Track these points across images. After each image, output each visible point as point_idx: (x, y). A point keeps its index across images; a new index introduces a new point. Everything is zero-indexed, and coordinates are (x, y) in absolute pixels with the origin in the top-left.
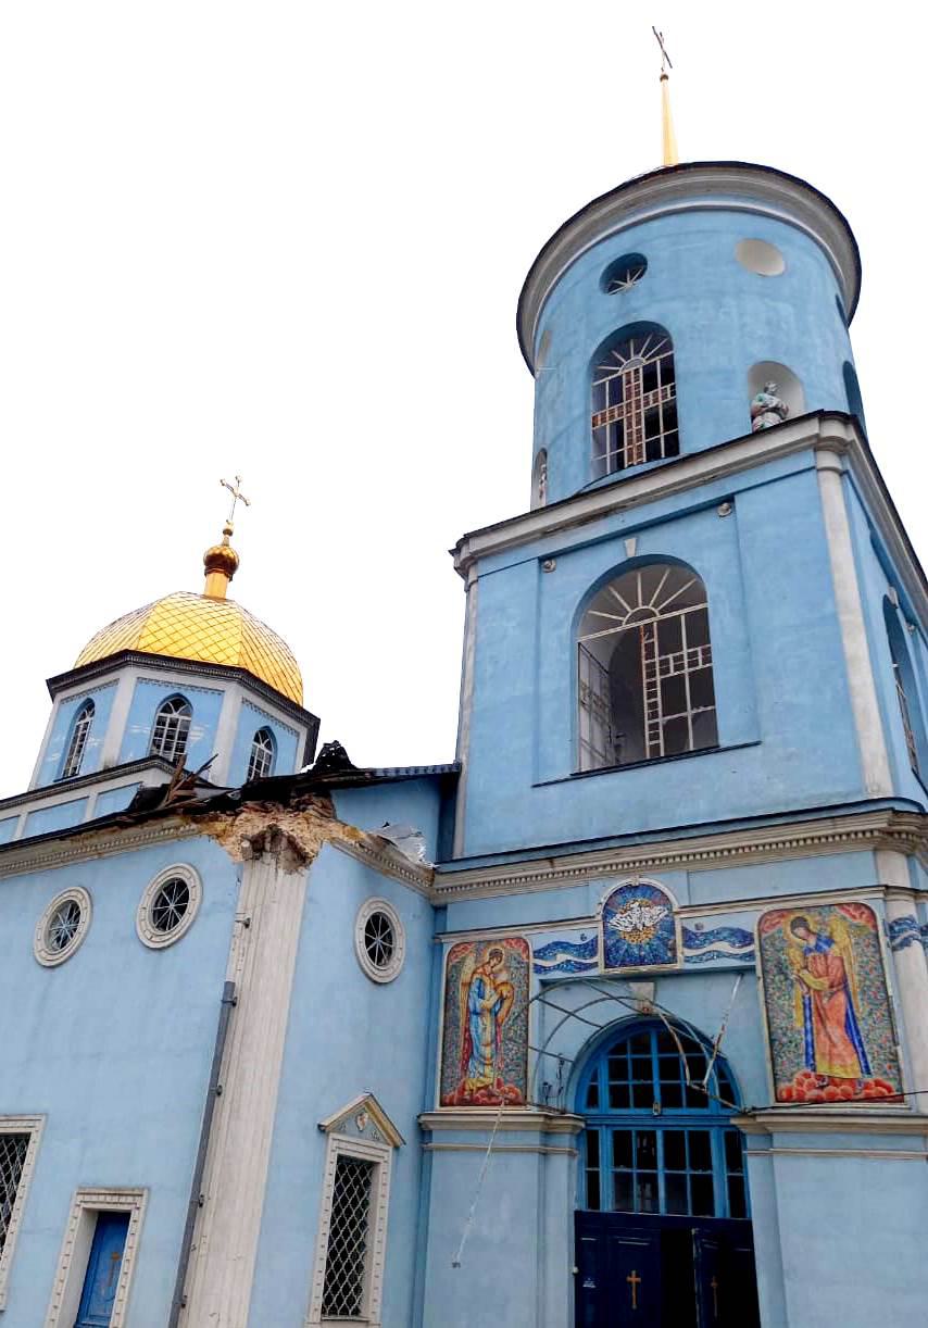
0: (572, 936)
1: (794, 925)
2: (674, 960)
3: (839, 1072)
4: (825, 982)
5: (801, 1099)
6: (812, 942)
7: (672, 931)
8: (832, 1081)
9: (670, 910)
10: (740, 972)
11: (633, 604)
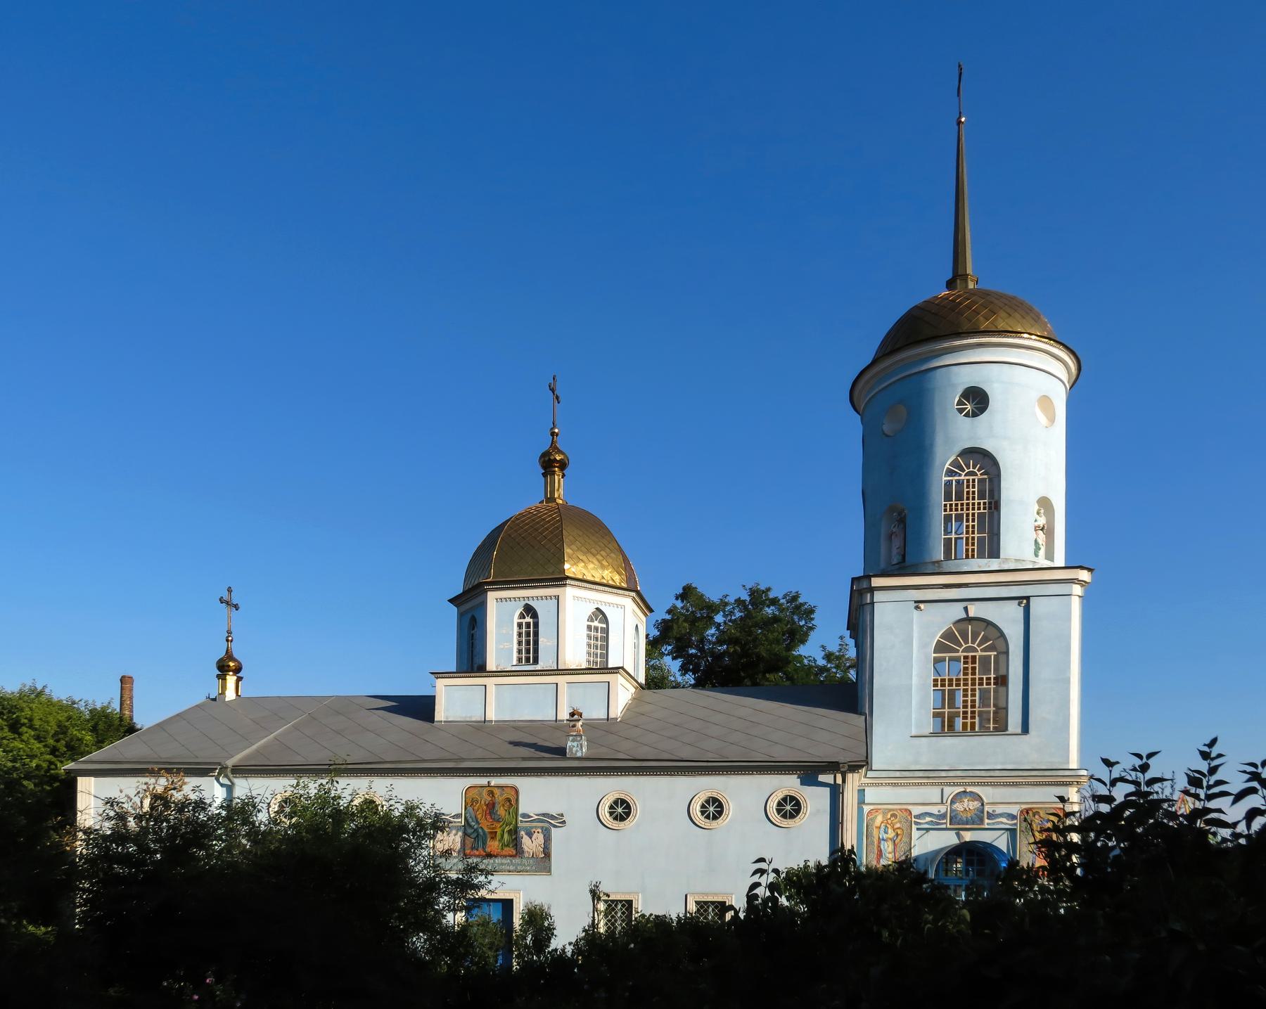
11: (966, 642)
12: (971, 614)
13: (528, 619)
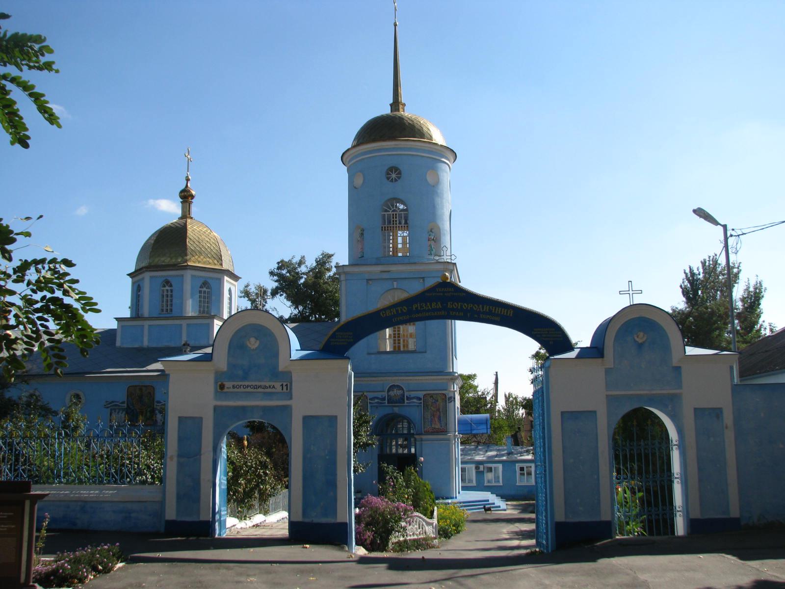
0: (379, 395)
1: (430, 397)
2: (404, 403)
3: (437, 427)
4: (435, 409)
5: (429, 432)
6: (434, 401)
7: (404, 397)
8: (435, 428)
9: (404, 391)
10: (418, 406)
12: (395, 287)
13: (167, 288)
